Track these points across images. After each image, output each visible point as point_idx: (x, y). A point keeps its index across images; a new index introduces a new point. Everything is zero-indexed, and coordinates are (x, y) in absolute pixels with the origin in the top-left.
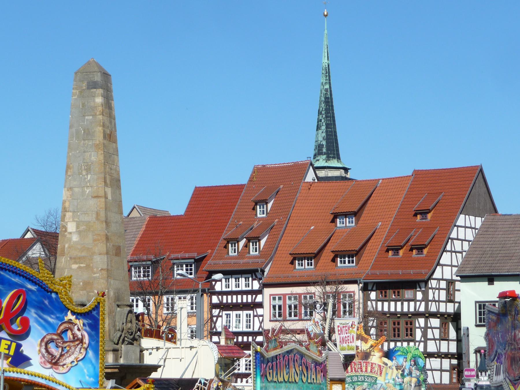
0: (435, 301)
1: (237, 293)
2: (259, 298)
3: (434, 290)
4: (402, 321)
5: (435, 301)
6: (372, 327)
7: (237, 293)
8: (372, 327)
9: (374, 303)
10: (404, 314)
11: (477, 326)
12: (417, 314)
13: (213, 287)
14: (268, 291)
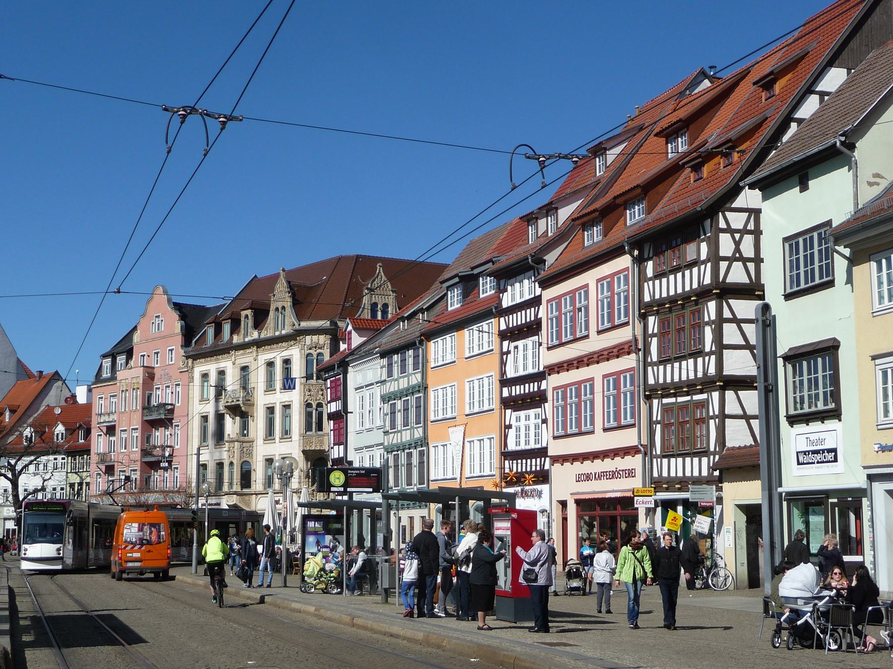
0: (745, 260)
3: (737, 236)
5: (745, 260)
6: (654, 335)
8: (654, 335)
9: (651, 283)
11: (788, 297)
12: (703, 294)
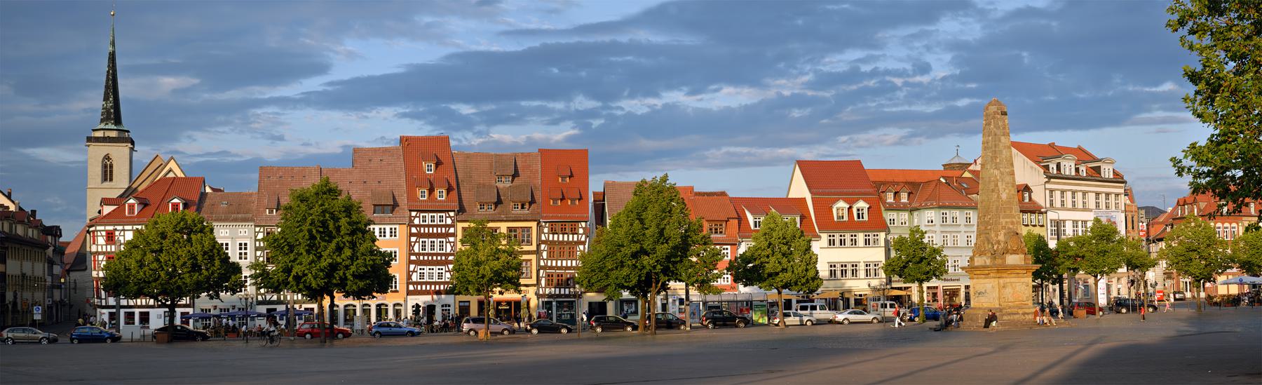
1: (433, 226)
2: (452, 230)
4: (567, 248)
7: (433, 226)
10: (568, 243)
13: (411, 221)
14: (460, 226)
